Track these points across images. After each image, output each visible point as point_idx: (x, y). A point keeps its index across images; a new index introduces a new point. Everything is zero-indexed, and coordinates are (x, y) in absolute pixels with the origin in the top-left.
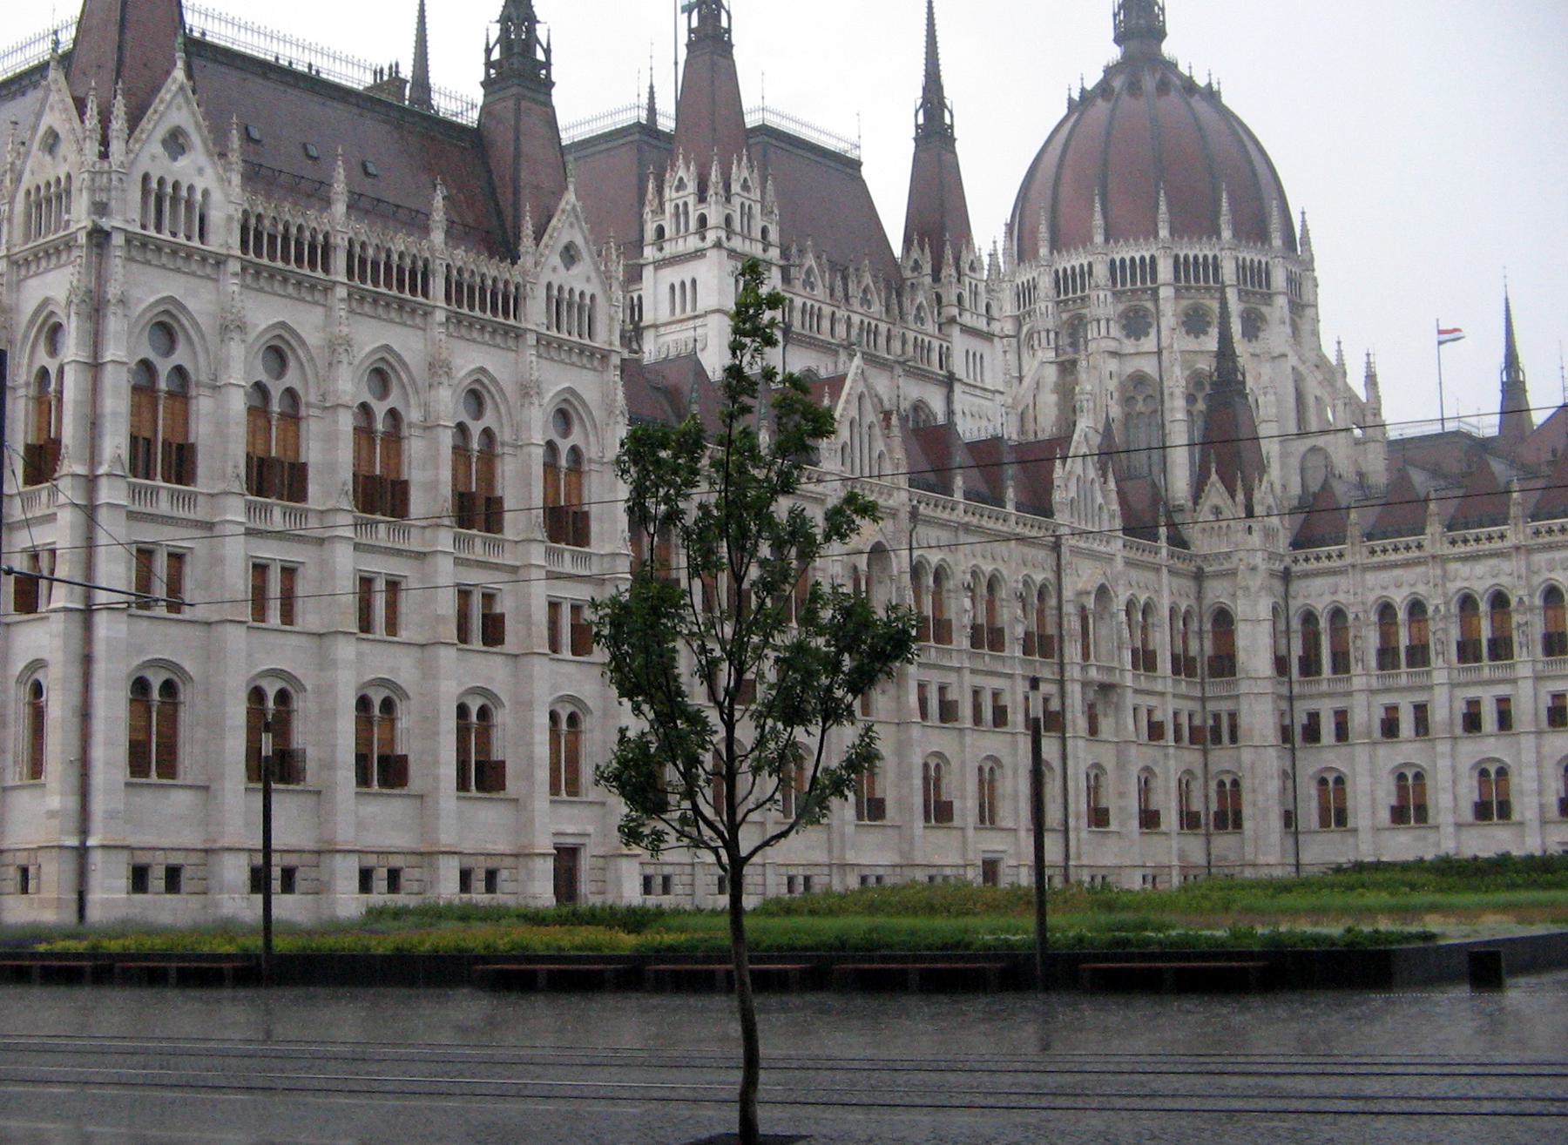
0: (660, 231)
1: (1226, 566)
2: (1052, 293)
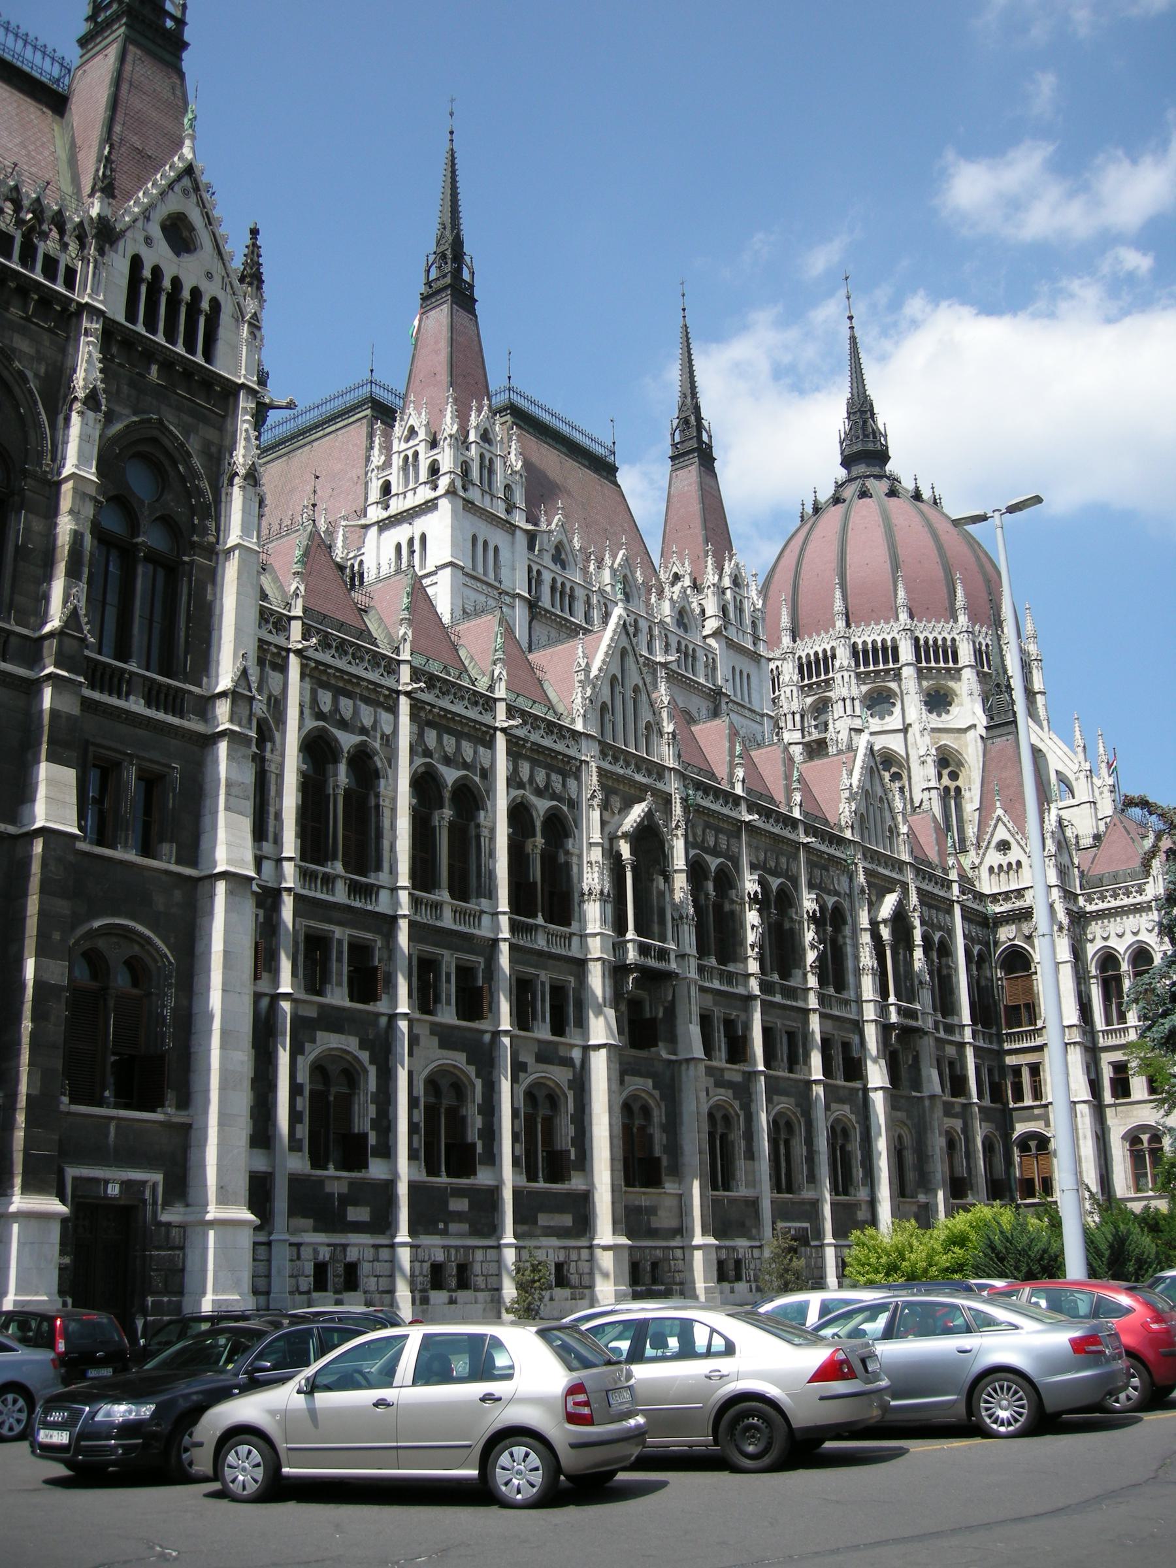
0: (386, 489)
1: (1019, 904)
2: (796, 677)
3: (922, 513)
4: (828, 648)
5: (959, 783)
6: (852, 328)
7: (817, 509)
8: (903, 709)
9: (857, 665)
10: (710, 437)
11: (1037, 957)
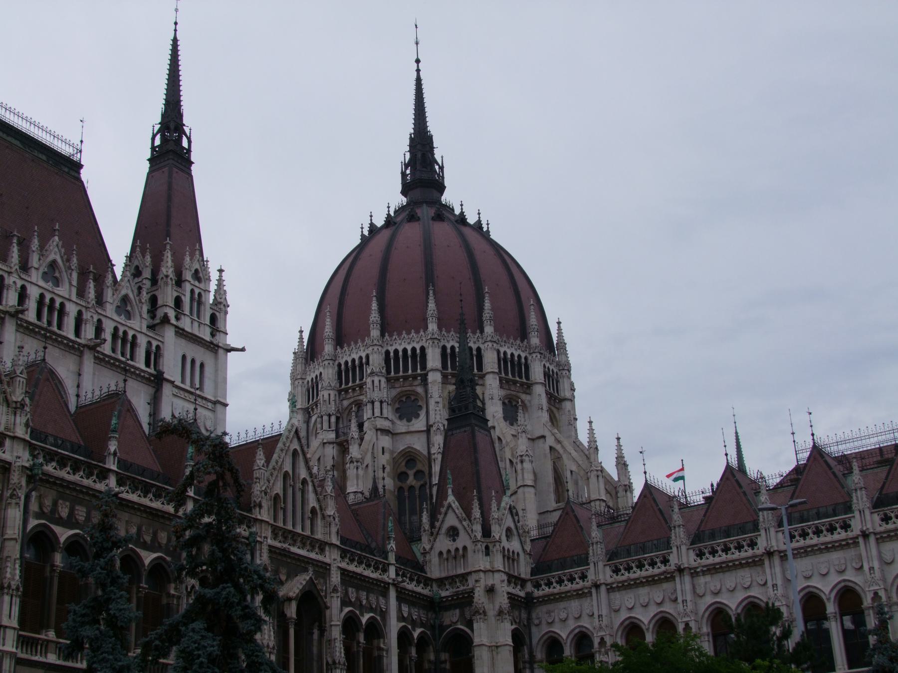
2: (335, 383)
3: (462, 236)
4: (364, 355)
6: (418, 71)
7: (370, 231)
8: (427, 413)
9: (389, 372)
10: (190, 142)
11: (476, 641)
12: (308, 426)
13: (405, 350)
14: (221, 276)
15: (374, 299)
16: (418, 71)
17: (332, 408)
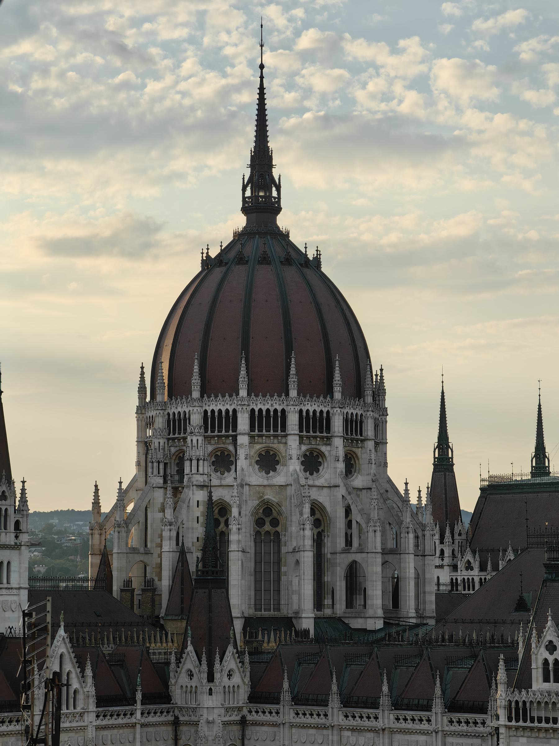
1: (193, 718)
5: (279, 529)
6: (262, 77)
9: (206, 431)
12: (146, 457)
13: (220, 411)
14: (23, 486)
15: (196, 361)
16: (262, 77)
17: (160, 456)
